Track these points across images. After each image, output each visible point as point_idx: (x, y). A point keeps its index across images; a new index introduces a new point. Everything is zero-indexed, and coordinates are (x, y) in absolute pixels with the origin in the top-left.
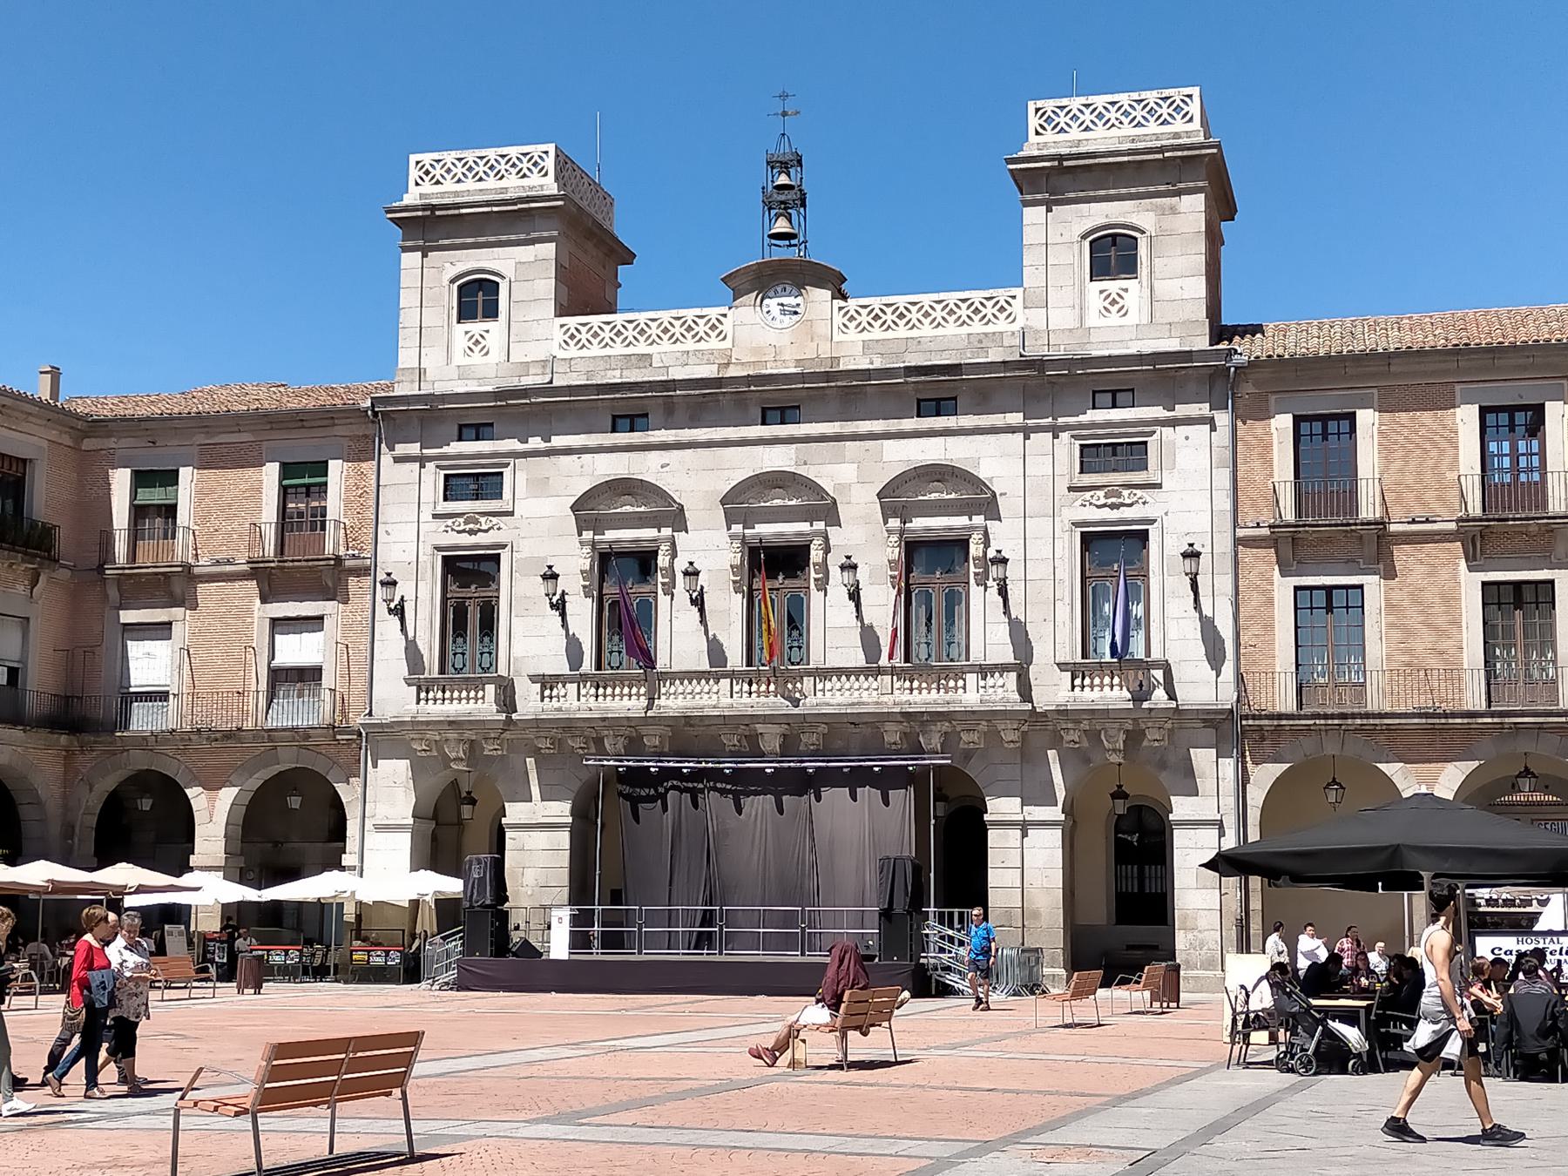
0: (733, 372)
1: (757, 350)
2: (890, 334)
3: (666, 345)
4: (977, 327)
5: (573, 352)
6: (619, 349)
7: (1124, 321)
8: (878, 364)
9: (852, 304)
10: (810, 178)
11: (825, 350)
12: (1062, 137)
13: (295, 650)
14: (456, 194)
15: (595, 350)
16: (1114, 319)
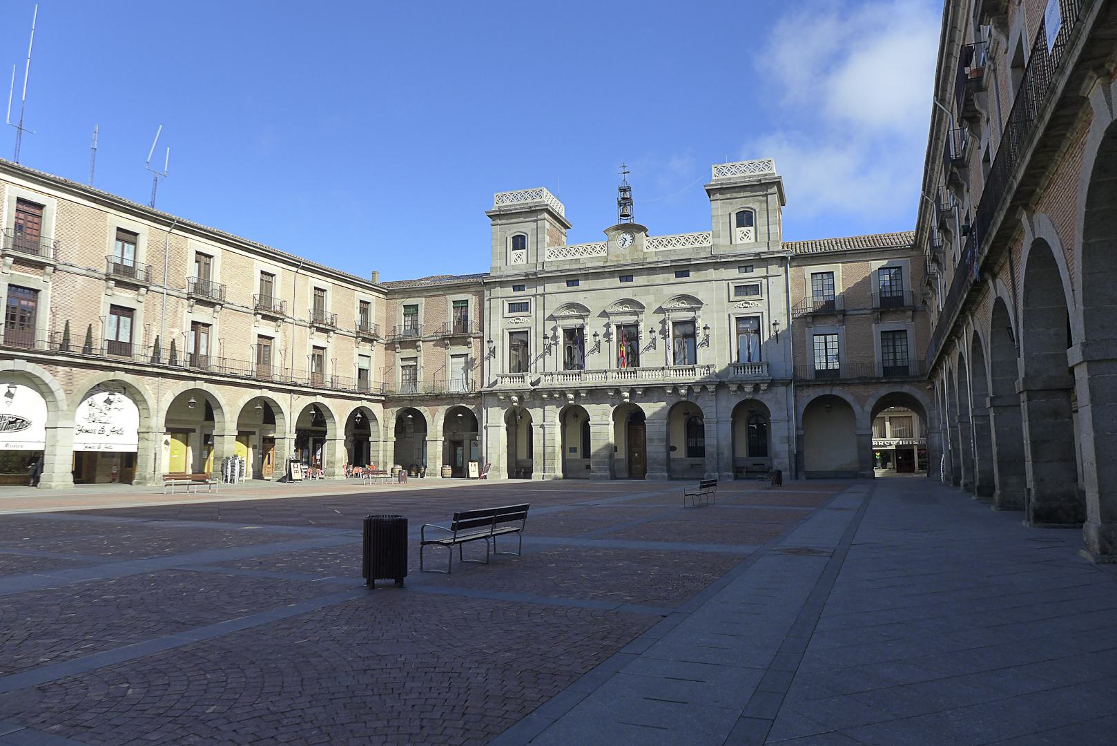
1: (617, 256)
3: (586, 256)
4: (697, 245)
5: (553, 258)
6: (569, 257)
8: (661, 259)
9: (650, 239)
10: (634, 195)
12: (725, 177)
14: (510, 206)
15: (561, 258)
16: (746, 241)
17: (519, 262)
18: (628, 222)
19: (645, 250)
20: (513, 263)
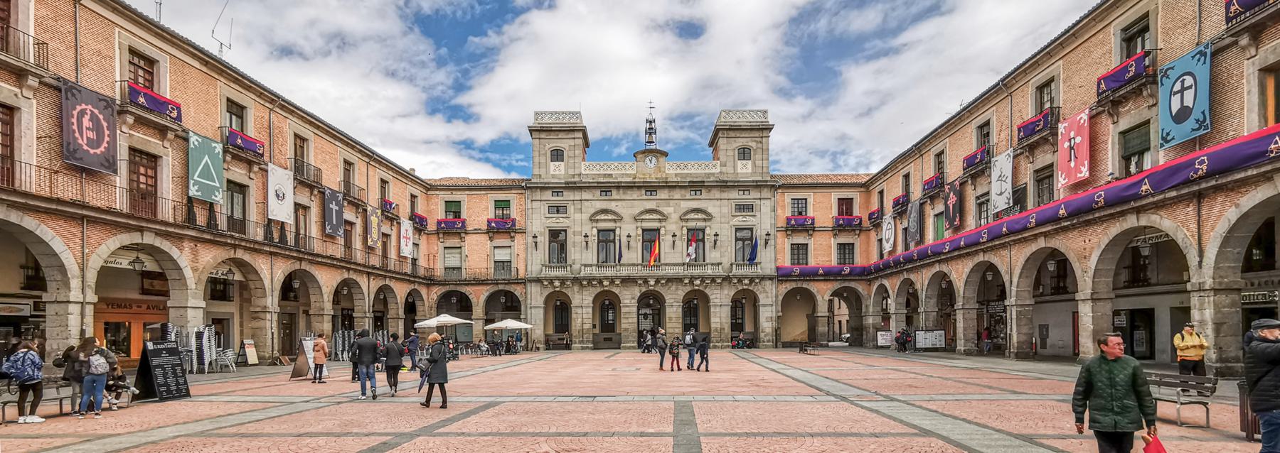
0: (637, 180)
1: (644, 174)
2: (682, 172)
5: (588, 172)
6: (602, 172)
7: (748, 171)
11: (664, 176)
13: (502, 255)
17: (557, 172)
18: (654, 147)
19: (667, 172)
20: (552, 172)
